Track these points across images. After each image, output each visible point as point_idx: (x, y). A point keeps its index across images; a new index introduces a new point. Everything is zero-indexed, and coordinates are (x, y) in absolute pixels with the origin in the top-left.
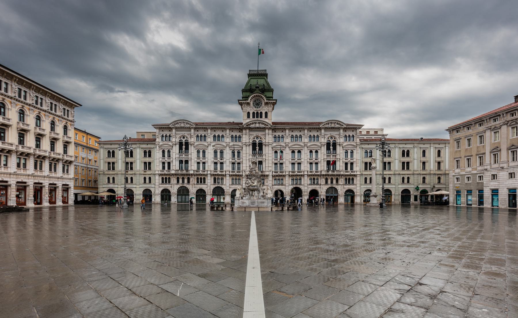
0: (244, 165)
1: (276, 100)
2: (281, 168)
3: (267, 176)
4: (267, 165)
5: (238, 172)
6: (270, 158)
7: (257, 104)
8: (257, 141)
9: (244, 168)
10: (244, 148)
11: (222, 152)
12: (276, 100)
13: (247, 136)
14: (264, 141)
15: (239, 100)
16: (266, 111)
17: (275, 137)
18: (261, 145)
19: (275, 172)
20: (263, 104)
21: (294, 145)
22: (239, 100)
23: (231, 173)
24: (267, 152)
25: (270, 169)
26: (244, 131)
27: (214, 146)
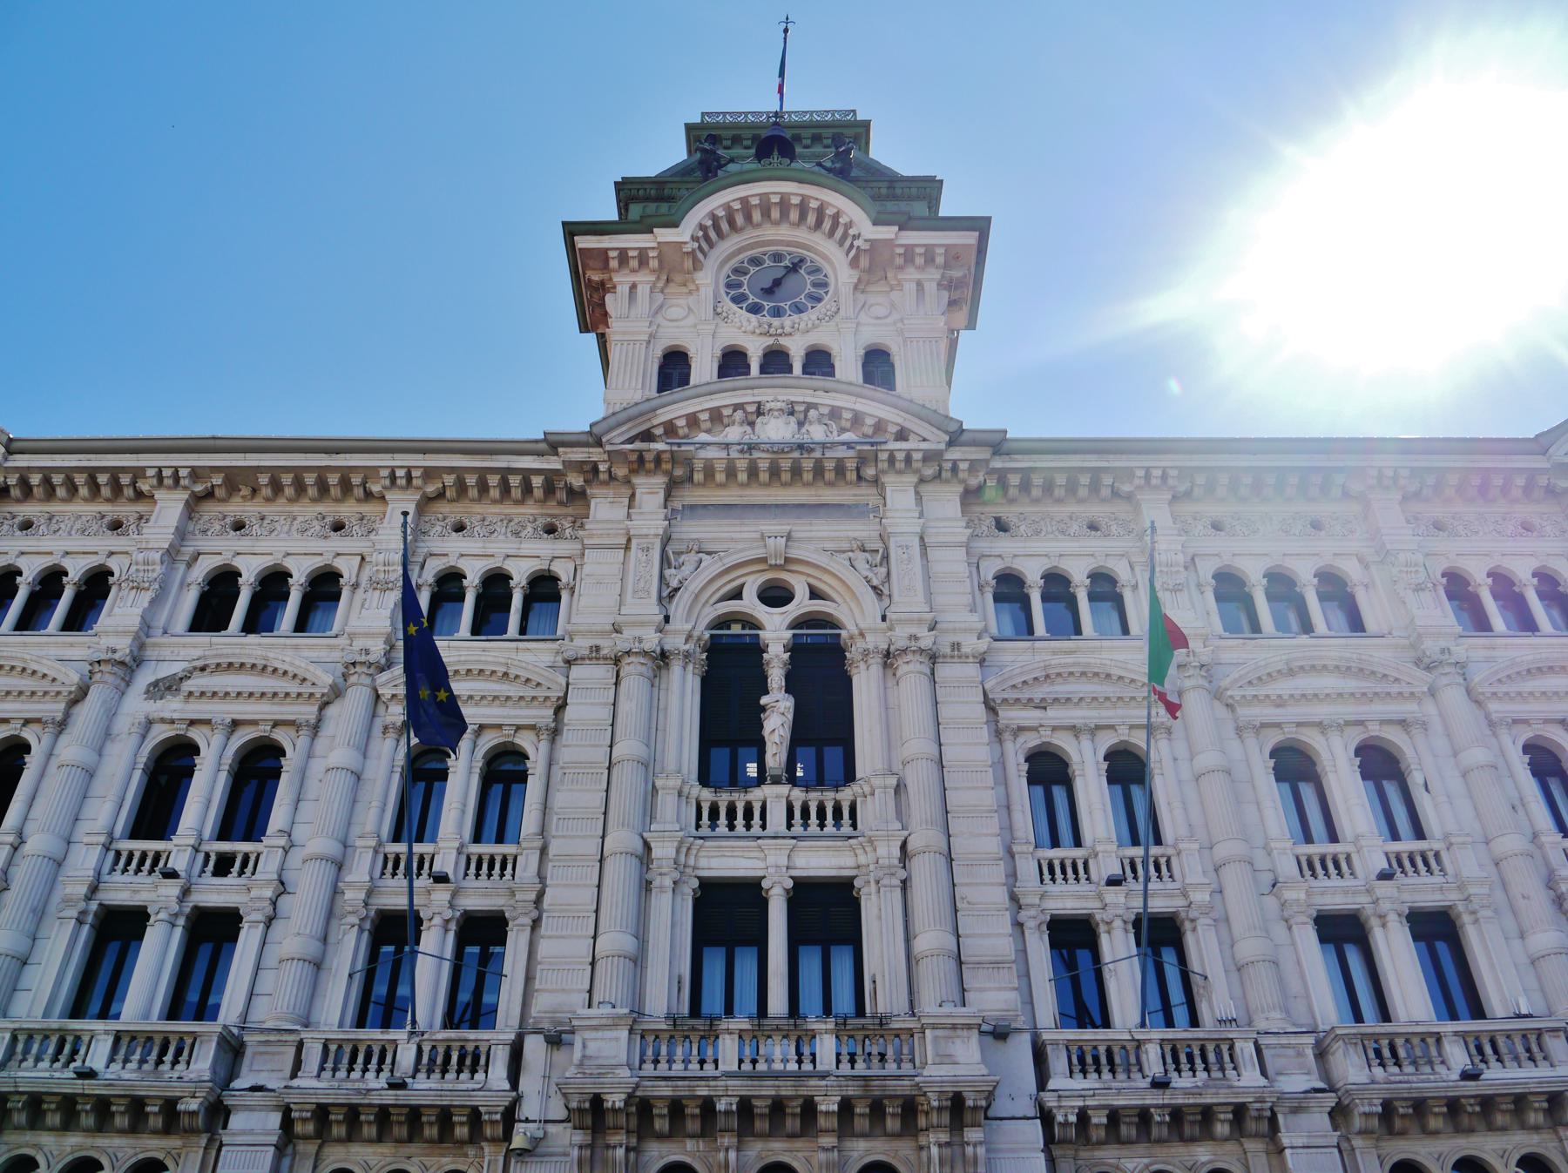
0: (562, 946)
1: (980, 226)
2: (1174, 991)
3: (959, 1111)
4: (931, 939)
5: (436, 1062)
6: (978, 840)
7: (776, 284)
8: (776, 629)
9: (560, 995)
10: (585, 711)
11: (258, 769)
12: (980, 226)
13: (646, 566)
14: (857, 617)
15: (572, 230)
16: (872, 334)
17: (1009, 588)
18: (822, 665)
19: (1084, 1062)
20: (842, 275)
21: (1291, 673)
22: (572, 230)
23: (315, 1085)
24: (917, 744)
25: (993, 997)
26: (604, 508)
27: (164, 688)
